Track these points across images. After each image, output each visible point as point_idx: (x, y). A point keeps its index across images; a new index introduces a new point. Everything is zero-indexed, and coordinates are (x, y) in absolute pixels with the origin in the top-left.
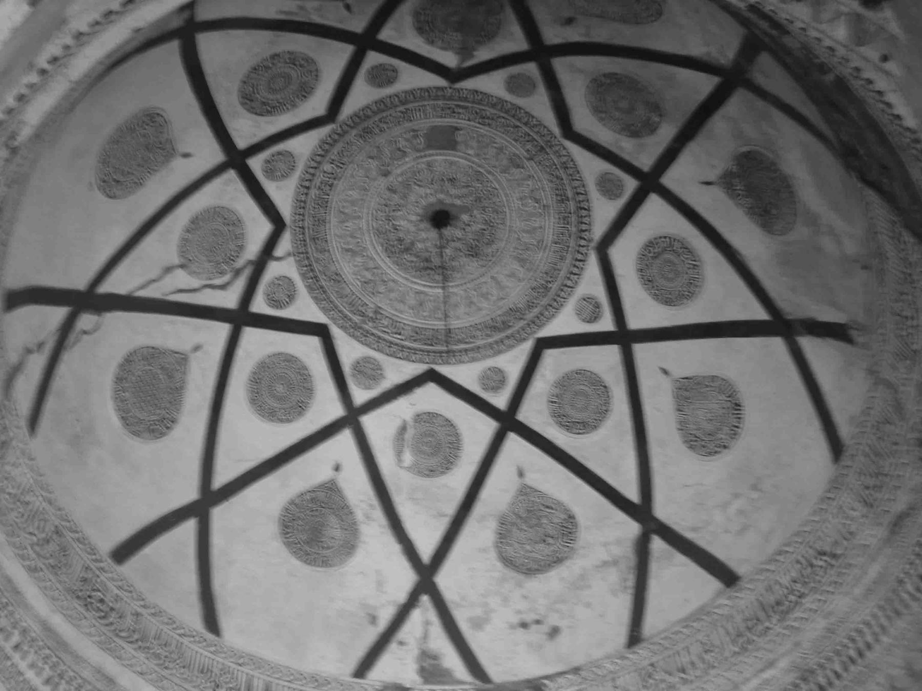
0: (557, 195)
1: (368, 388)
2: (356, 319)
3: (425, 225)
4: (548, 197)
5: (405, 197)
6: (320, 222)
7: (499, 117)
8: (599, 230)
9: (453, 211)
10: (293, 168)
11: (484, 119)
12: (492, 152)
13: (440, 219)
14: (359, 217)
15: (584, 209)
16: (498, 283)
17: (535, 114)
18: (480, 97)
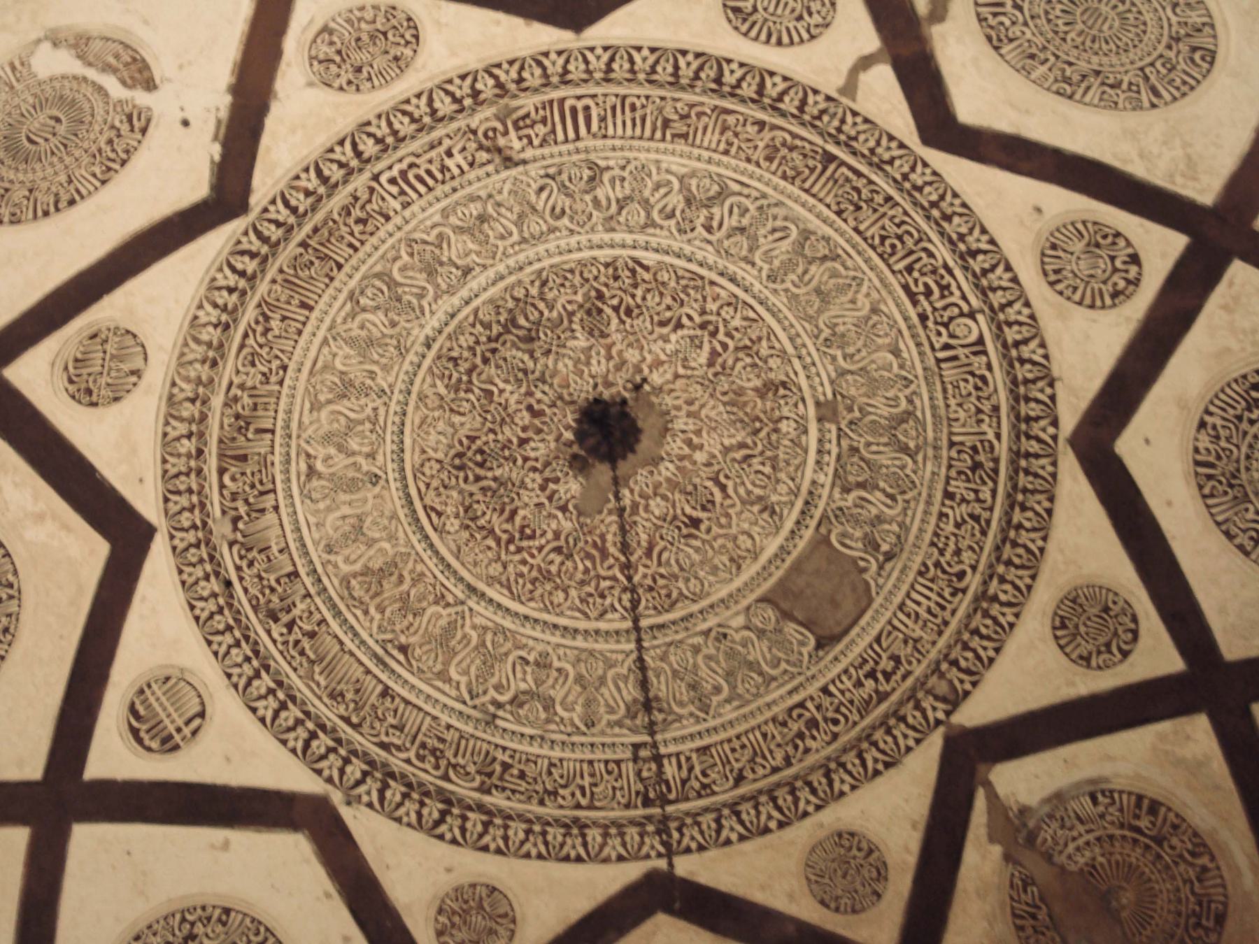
0: (506, 767)
1: (326, 29)
2: (528, 103)
3: (620, 387)
4: (516, 737)
5: (736, 399)
6: (851, 205)
7: (788, 761)
8: (369, 829)
9: (602, 472)
10: (1054, 279)
11: (805, 722)
12: (709, 677)
13: (608, 431)
14: (772, 278)
15: (442, 816)
16: (352, 486)
17: (747, 846)
18: (873, 759)
